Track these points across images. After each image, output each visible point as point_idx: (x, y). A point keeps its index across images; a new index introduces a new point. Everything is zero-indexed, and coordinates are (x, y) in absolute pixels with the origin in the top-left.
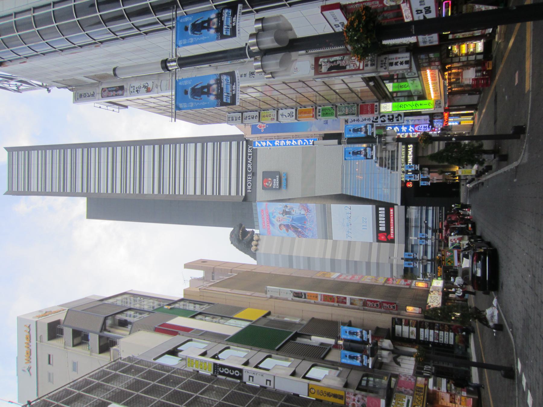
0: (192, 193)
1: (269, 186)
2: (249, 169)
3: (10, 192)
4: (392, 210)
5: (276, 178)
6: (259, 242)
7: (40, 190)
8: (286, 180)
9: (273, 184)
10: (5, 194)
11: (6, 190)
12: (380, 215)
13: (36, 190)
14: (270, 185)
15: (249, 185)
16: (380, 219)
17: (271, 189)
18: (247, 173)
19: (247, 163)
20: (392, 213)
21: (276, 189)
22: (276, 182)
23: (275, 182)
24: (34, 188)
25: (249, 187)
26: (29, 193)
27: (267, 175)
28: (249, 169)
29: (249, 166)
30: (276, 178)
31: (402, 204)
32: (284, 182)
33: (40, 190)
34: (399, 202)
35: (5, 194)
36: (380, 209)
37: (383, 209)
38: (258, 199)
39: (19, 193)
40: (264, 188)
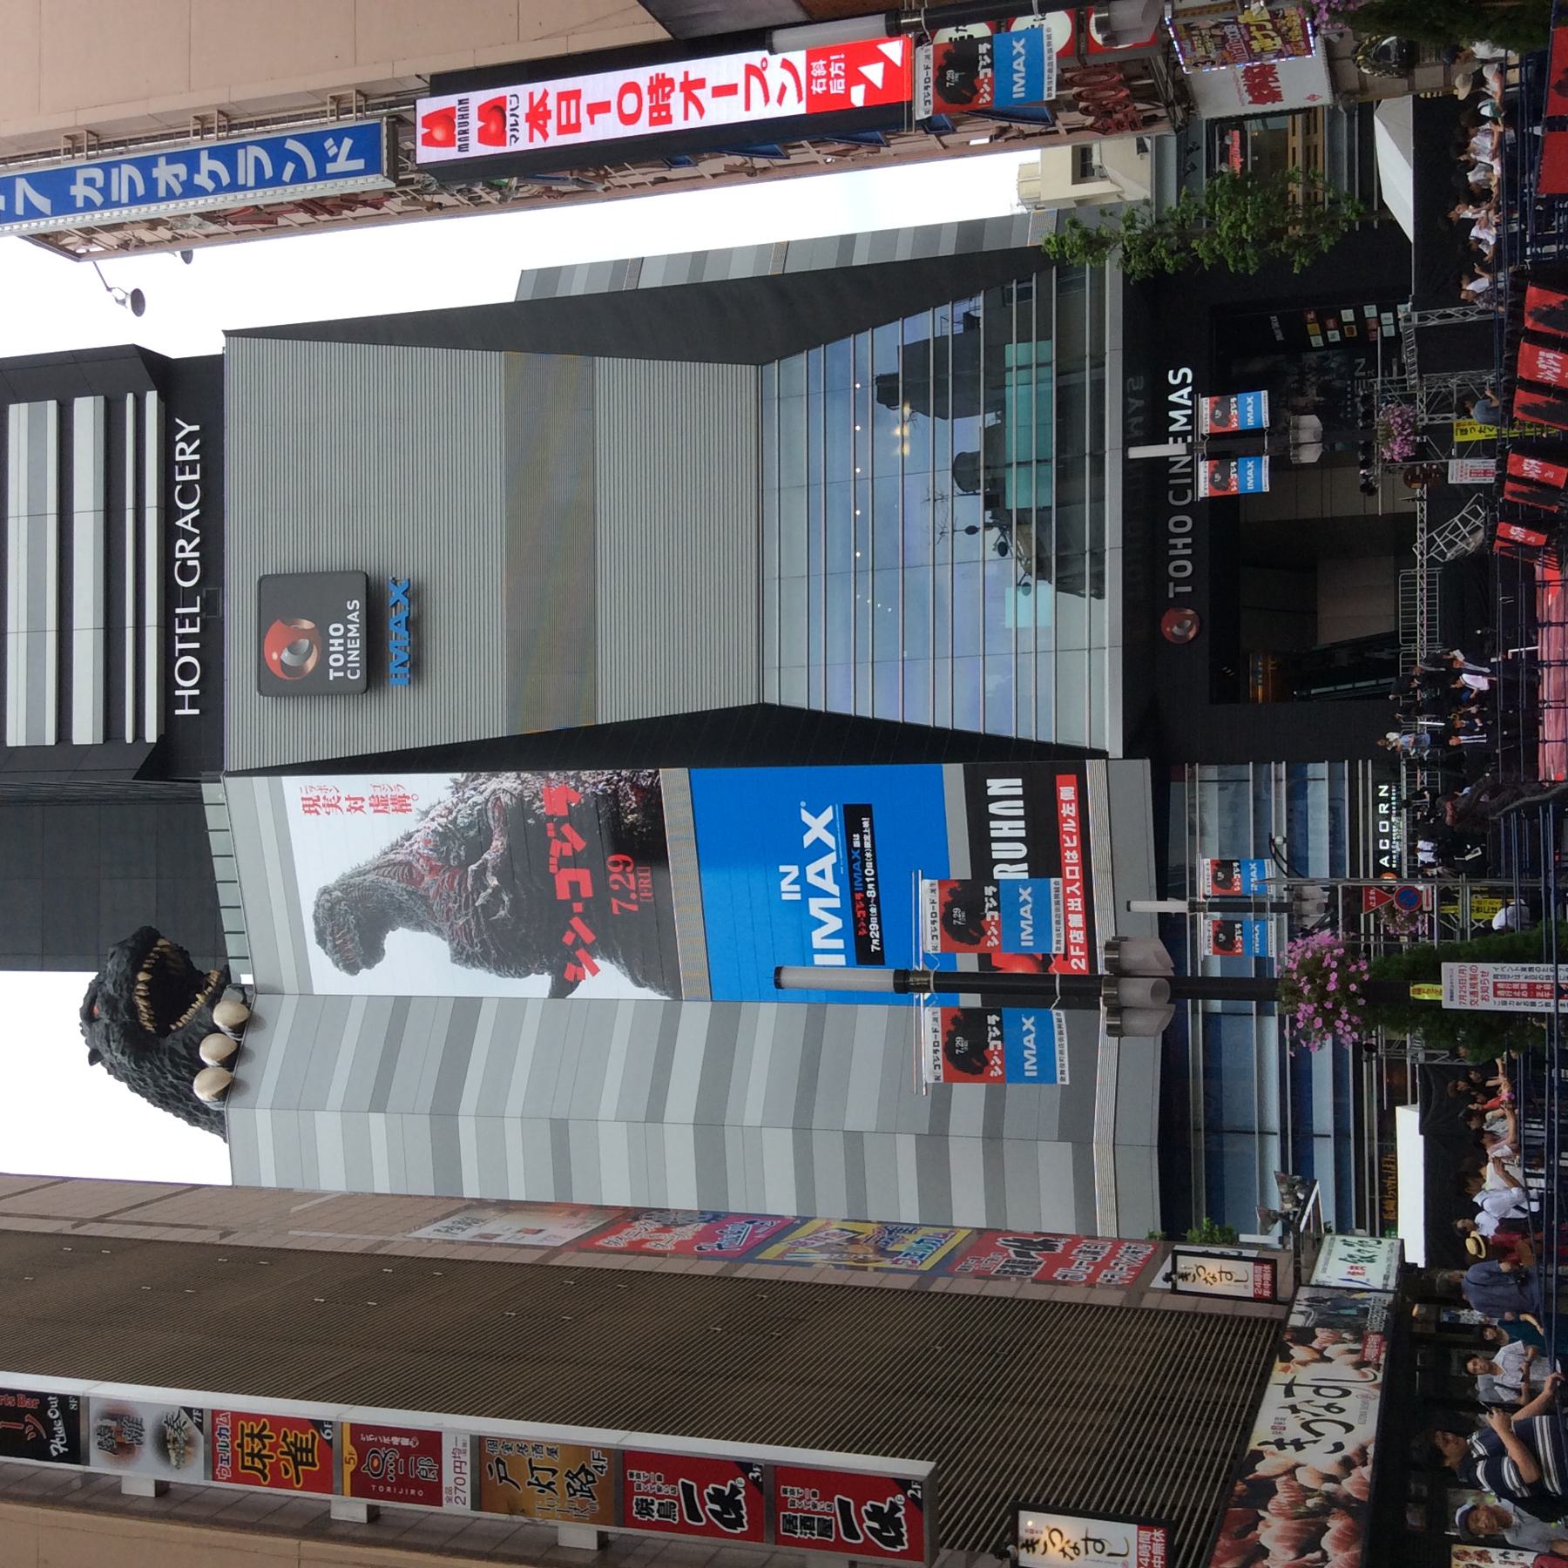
1: (297, 670)
2: (186, 573)
4: (1067, 793)
8: (414, 625)
9: (325, 654)
12: (999, 829)
14: (311, 664)
15: (187, 671)
16: (999, 851)
19: (169, 534)
20: (1068, 810)
21: (339, 690)
22: (345, 645)
28: (186, 573)
31: (1130, 752)
34: (1112, 739)
36: (995, 786)
37: (1013, 786)
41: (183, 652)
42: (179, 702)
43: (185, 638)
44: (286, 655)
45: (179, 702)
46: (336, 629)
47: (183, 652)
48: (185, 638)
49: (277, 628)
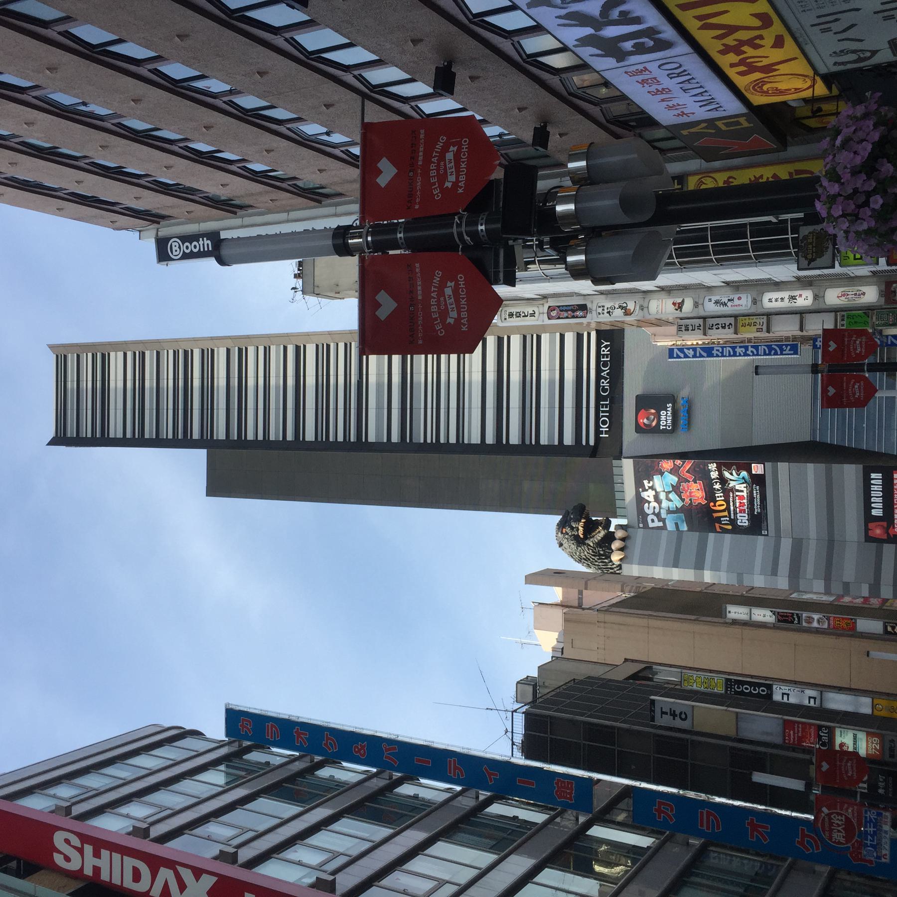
0: (476, 439)
1: (649, 425)
2: (605, 390)
3: (60, 439)
5: (666, 409)
6: (628, 542)
7: (129, 435)
8: (689, 412)
9: (659, 421)
10: (50, 444)
11: (51, 434)
13: (120, 435)
14: (654, 424)
15: (604, 422)
17: (656, 430)
18: (598, 398)
22: (666, 418)
23: (663, 418)
24: (115, 430)
25: (604, 428)
26: (104, 440)
27: (644, 402)
28: (605, 390)
29: (605, 383)
30: (666, 409)
32: (682, 415)
33: (129, 435)
35: (50, 444)
38: (624, 454)
39: (79, 441)
40: (639, 429)
41: (603, 416)
42: (602, 432)
43: (603, 412)
44: (645, 421)
45: (602, 432)
46: (663, 413)
47: (603, 416)
48: (603, 412)
49: (642, 412)
